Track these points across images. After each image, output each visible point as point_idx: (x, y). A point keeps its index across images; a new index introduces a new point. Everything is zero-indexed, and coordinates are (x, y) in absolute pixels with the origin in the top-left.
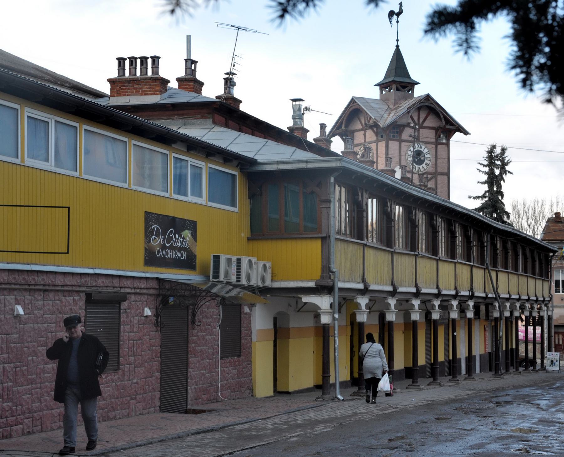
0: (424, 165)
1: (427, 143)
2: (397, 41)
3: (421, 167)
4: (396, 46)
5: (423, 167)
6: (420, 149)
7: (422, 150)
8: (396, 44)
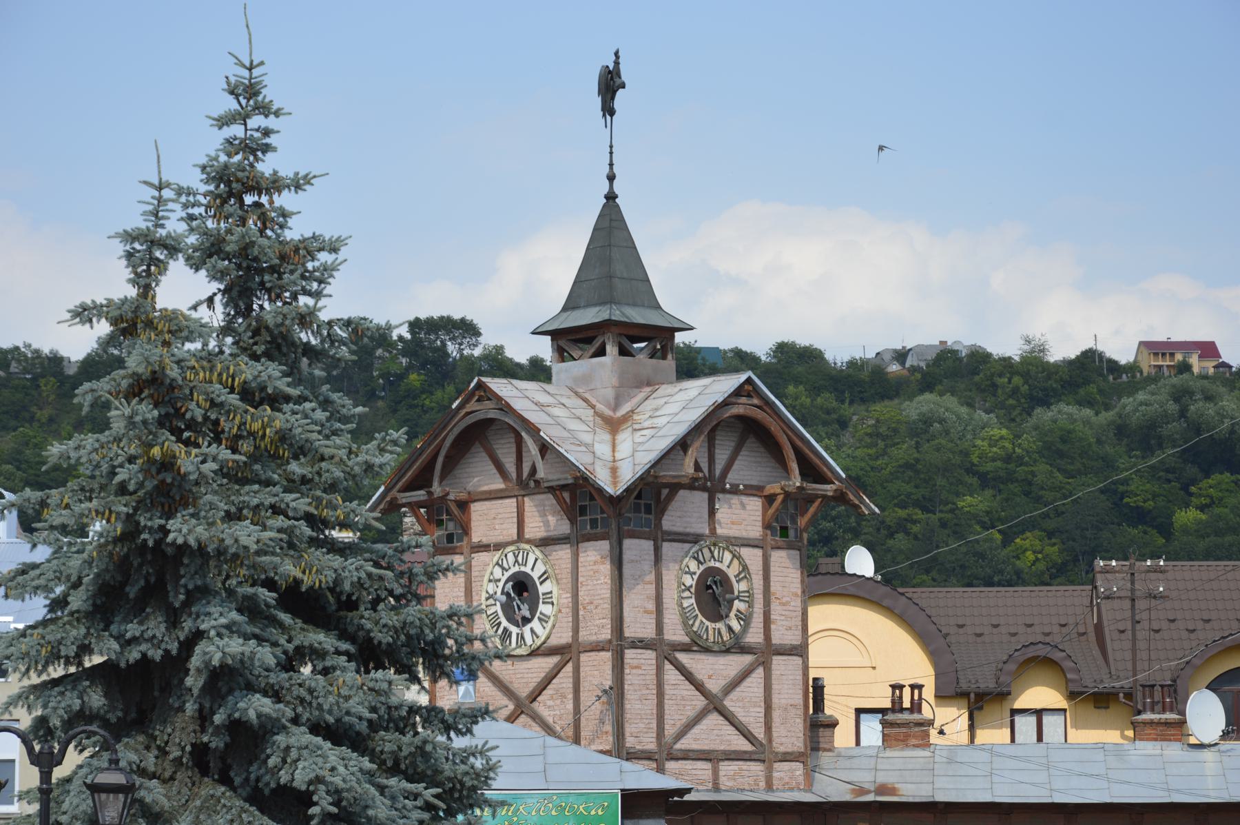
0: (535, 624)
2: (611, 178)
3: (527, 629)
5: (532, 631)
6: (523, 569)
7: (527, 569)
8: (605, 189)
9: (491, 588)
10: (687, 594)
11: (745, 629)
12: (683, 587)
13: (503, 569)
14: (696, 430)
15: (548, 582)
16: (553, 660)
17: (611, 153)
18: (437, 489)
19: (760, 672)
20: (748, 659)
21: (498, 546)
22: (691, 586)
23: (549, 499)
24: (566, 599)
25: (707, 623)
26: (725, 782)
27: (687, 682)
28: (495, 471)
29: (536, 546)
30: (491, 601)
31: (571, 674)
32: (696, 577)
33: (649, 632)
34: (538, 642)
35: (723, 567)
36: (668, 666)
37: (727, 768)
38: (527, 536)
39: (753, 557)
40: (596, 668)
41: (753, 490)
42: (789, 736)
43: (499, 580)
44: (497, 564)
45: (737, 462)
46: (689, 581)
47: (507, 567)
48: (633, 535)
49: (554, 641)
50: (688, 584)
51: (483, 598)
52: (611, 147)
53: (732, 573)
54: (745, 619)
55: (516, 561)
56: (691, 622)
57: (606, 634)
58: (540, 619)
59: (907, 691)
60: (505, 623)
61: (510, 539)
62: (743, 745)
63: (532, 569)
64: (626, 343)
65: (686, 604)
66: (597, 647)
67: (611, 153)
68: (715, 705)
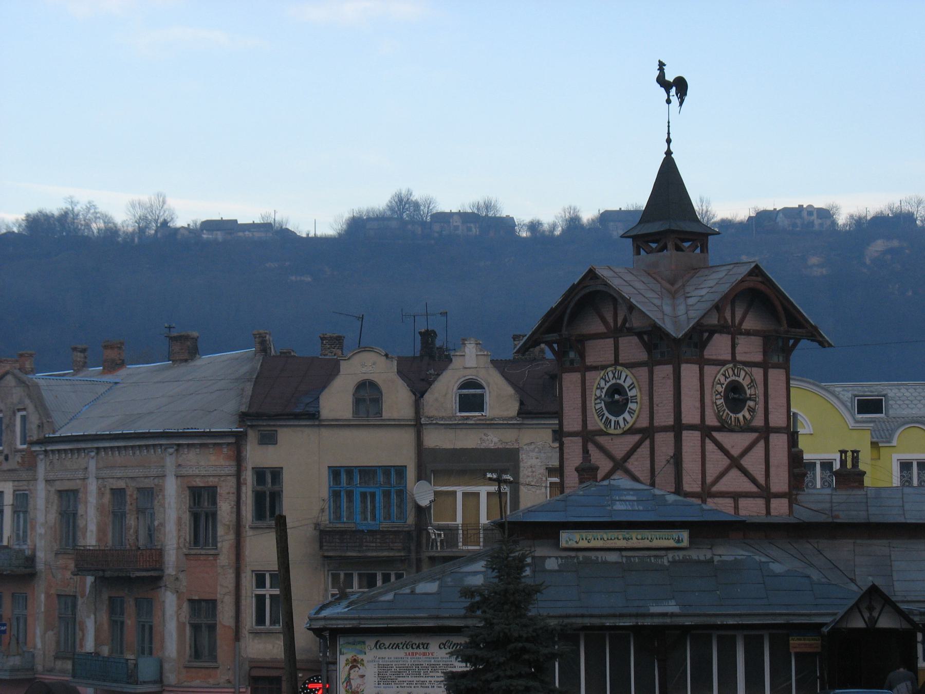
0: (626, 415)
1: (630, 366)
2: (669, 141)
3: (620, 419)
4: (666, 153)
5: (624, 419)
6: (618, 381)
7: (621, 382)
8: (666, 149)
9: (598, 393)
10: (718, 396)
11: (753, 417)
12: (717, 393)
13: (606, 381)
14: (725, 297)
15: (634, 389)
16: (637, 437)
17: (669, 126)
18: (564, 332)
19: (762, 444)
20: (754, 435)
21: (604, 367)
22: (721, 392)
23: (635, 340)
24: (646, 399)
25: (731, 414)
26: (743, 512)
27: (719, 451)
28: (600, 322)
29: (627, 368)
30: (598, 401)
31: (649, 446)
32: (724, 386)
33: (696, 420)
34: (628, 426)
35: (740, 380)
36: (708, 441)
37: (743, 502)
38: (620, 362)
39: (758, 373)
40: (665, 443)
41: (756, 333)
42: (780, 481)
43: (603, 388)
44: (602, 378)
45: (748, 316)
46: (720, 389)
48: (687, 362)
49: (638, 425)
50: (720, 391)
51: (593, 399)
52: (669, 122)
53: (745, 383)
54: (752, 410)
55: (614, 376)
56: (721, 414)
57: (670, 421)
58: (628, 411)
59: (849, 454)
60: (607, 414)
61: (609, 363)
62: (754, 489)
63: (624, 382)
64: (679, 242)
65: (719, 402)
66: (665, 429)
67: (669, 126)
68: (735, 463)
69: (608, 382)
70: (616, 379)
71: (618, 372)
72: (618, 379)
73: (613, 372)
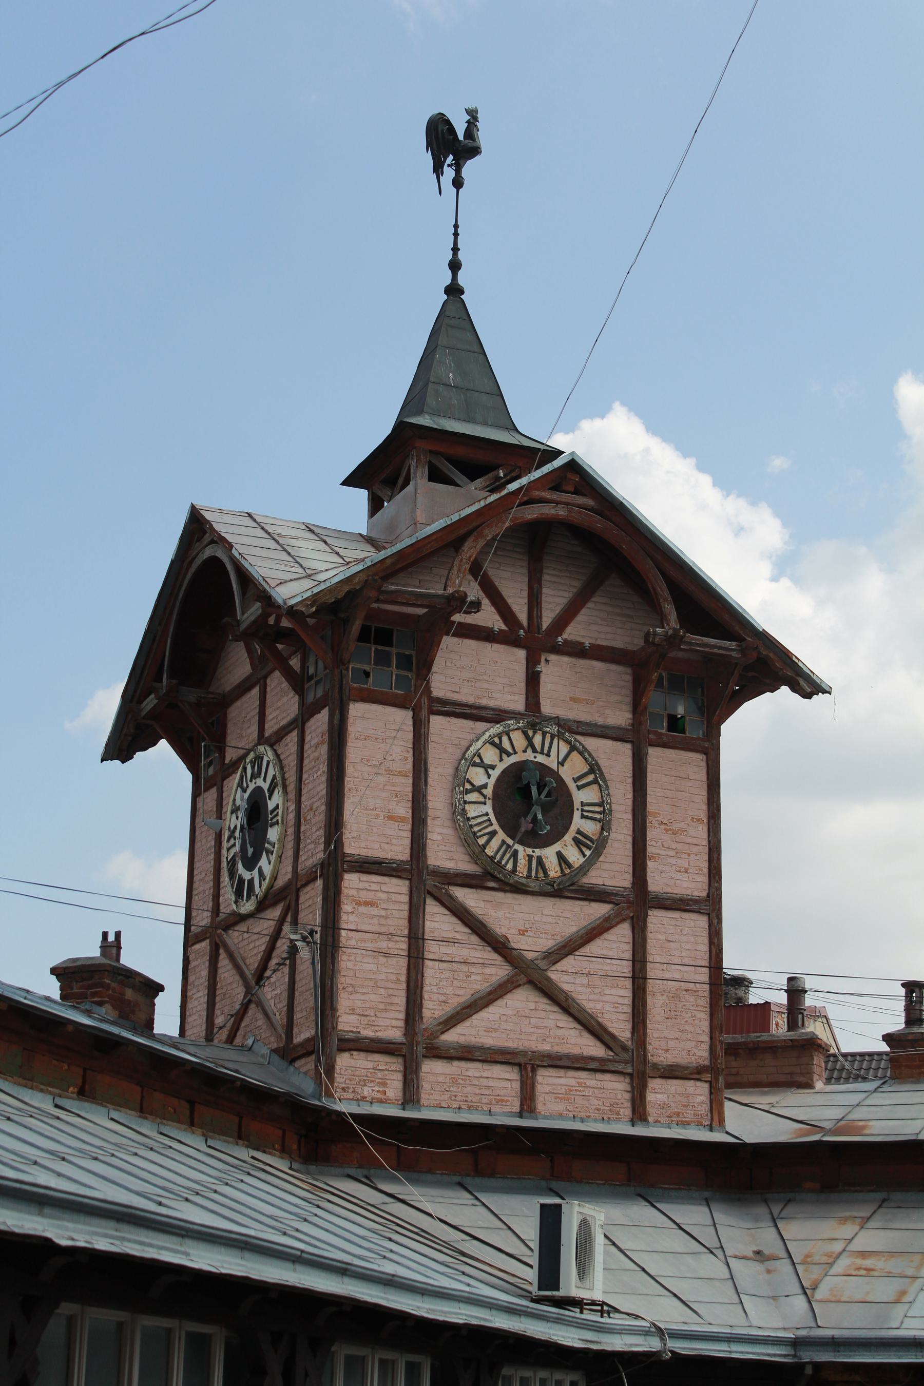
2: (455, 266)
7: (551, 762)
13: (503, 751)
17: (456, 235)
43: (493, 767)
47: (510, 750)
52: (456, 226)
63: (561, 763)
67: (456, 235)
69: (509, 755)
70: (534, 750)
71: (544, 734)
72: (542, 753)
73: (525, 734)
